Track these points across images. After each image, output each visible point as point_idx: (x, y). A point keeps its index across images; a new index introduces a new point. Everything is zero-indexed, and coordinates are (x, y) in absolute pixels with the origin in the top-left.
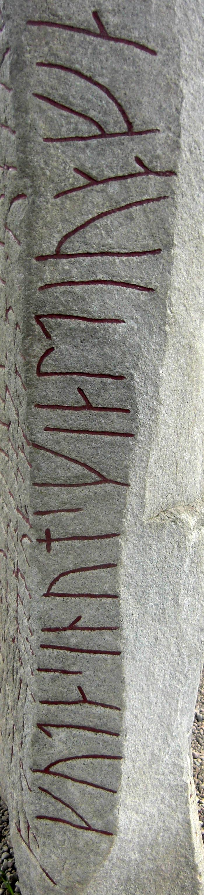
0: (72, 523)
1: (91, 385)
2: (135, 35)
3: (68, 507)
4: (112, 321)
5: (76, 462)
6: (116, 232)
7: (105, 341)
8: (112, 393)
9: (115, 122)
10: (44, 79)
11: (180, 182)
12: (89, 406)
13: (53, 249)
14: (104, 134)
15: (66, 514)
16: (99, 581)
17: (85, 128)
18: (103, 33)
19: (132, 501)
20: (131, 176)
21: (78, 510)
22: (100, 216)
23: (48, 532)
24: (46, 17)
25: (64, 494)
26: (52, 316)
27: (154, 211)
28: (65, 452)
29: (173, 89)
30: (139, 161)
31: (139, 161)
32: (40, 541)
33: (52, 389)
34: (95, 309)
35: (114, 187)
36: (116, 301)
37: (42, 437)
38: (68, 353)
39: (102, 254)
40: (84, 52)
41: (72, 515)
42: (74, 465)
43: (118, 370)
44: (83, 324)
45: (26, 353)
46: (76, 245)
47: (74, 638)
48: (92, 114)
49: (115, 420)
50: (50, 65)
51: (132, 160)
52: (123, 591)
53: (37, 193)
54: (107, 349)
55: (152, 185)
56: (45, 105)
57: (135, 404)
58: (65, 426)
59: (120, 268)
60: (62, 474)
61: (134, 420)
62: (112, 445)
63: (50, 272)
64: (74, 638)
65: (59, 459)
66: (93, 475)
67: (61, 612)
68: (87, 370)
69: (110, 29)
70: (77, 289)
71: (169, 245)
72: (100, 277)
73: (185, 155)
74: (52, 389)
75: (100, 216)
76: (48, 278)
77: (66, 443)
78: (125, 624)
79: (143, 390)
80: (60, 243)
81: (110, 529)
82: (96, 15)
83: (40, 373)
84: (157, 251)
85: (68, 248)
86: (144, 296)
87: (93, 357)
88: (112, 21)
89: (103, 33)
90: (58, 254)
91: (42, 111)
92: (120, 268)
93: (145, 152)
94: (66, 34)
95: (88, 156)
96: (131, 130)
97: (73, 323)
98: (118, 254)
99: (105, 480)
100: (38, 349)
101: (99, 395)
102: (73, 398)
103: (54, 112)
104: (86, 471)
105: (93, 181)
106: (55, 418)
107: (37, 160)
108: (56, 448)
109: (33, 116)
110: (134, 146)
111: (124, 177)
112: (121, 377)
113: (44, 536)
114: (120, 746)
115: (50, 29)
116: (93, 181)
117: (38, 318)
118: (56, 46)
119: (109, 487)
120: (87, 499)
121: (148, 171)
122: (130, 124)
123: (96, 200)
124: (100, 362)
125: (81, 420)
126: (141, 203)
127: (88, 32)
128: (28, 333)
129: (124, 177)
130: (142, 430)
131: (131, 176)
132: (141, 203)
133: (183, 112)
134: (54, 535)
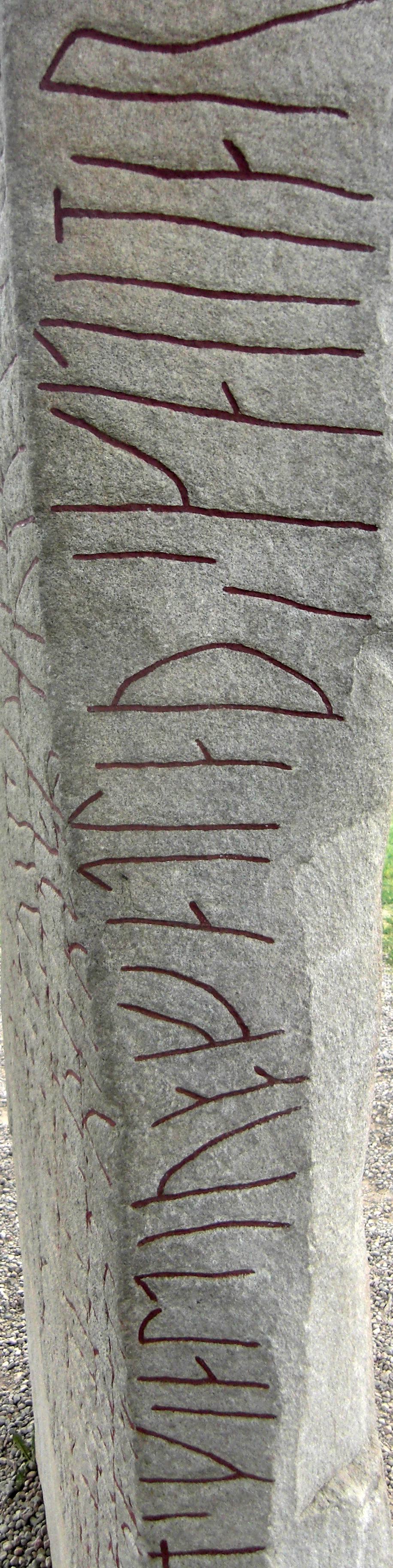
0: (197, 1533)
1: (213, 1355)
2: (245, 925)
3: (191, 1510)
4: (236, 1273)
5: (198, 1450)
6: (235, 1160)
7: (229, 1301)
8: (242, 1365)
10: (132, 986)
11: (315, 1084)
12: (212, 1379)
13: (154, 1191)
14: (212, 1044)
15: (188, 1520)
17: (188, 1039)
18: (205, 924)
20: (250, 1090)
21: (203, 1515)
22: (213, 1143)
23: (164, 1544)
24: (130, 913)
25: (185, 1495)
26: (157, 1275)
27: (284, 1128)
28: (183, 1439)
29: (298, 979)
30: (260, 1071)
31: (260, 1071)
32: (153, 1555)
33: (159, 1358)
34: (214, 1263)
35: (229, 1106)
36: (241, 1245)
37: (149, 1419)
38: (179, 1314)
39: (219, 1189)
40: (181, 950)
41: (197, 1522)
42: (195, 1455)
43: (249, 1337)
44: (199, 1282)
45: (124, 1317)
46: (183, 1182)
48: (196, 1020)
49: (250, 1400)
50: (138, 968)
51: (251, 1072)
53: (129, 1124)
54: (232, 1311)
55: (279, 1097)
56: (134, 1016)
57: (275, 1378)
58: (180, 1405)
59: (243, 1203)
60: (180, 1469)
61: (274, 1397)
62: (246, 1430)
63: (151, 1223)
65: (174, 1448)
66: (223, 1468)
68: (207, 1335)
69: (213, 919)
70: (189, 1239)
71: (307, 1165)
72: (218, 1219)
73: (320, 1050)
74: (159, 1358)
75: (213, 1143)
76: (149, 1229)
77: (183, 1427)
79: (284, 1357)
80: (163, 1182)
81: (250, 1542)
82: (194, 906)
83: (142, 1340)
84: (293, 1175)
85: (174, 1187)
86: (277, 1235)
87: (214, 1320)
88: (214, 911)
89: (205, 924)
90: (162, 1196)
91: (131, 1025)
92: (243, 1203)
93: (268, 1060)
94: (157, 930)
95: (194, 1073)
96: (247, 1036)
97: (185, 1282)
98: (241, 1187)
99: (239, 1474)
100: (140, 1312)
101: (225, 1367)
103: (147, 1024)
104: (213, 1464)
105: (202, 1100)
106: (166, 1394)
107: (128, 1085)
108: (171, 1434)
109: (120, 1032)
110: (251, 1055)
111: (242, 1092)
112: (254, 1344)
113: (158, 1549)
115: (136, 927)
116: (202, 1100)
117: (138, 1280)
118: (145, 946)
119: (247, 1484)
120: (216, 1502)
121: (272, 1081)
122: (245, 1029)
123: (207, 1123)
124: (224, 1326)
125: (202, 1396)
126: (266, 1119)
127: (186, 925)
128: (126, 1293)
129: (242, 1092)
130: (286, 1407)
131: (250, 1090)
132: (266, 1119)
133: (314, 1004)
134: (172, 1548)
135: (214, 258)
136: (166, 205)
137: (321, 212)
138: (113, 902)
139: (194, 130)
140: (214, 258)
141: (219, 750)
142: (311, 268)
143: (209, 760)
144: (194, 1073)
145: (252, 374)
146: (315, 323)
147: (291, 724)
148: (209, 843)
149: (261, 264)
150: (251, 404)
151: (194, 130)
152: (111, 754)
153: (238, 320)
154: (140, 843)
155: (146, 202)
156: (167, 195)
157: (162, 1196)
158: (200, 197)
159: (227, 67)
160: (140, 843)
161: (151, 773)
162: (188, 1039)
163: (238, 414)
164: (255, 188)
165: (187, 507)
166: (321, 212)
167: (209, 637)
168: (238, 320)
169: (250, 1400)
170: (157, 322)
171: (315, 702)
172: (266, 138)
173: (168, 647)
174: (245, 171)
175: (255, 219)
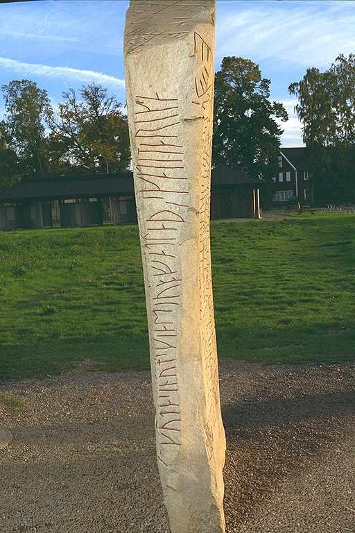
0: (164, 358)
1: (167, 326)
16: (172, 372)
17: (162, 273)
40: (159, 258)
46: (161, 295)
47: (166, 387)
59: (171, 300)
64: (166, 387)
67: (164, 380)
90: (157, 298)
92: (171, 300)
95: (162, 278)
102: (163, 329)
106: (160, 333)
123: (164, 287)
125: (166, 333)
135: (159, 156)
138: (150, 251)
139: (156, 140)
140: (159, 156)
142: (172, 157)
144: (162, 278)
151: (156, 140)
154: (155, 241)
157: (157, 298)
158: (158, 148)
159: (161, 132)
160: (155, 241)
162: (162, 273)
163: (166, 177)
168: (163, 164)
172: (166, 141)
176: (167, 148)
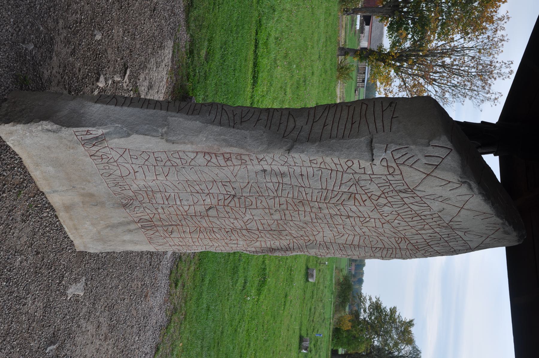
6: (225, 117)
9: (243, 120)
17: (243, 115)
19: (173, 114)
35: (232, 118)
36: (213, 116)
46: (223, 111)
52: (155, 111)
55: (232, 124)
59: (218, 117)
71: (221, 126)
78: (148, 110)
84: (220, 124)
85: (223, 111)
89: (258, 120)
90: (223, 109)
92: (218, 117)
96: (241, 122)
103: (247, 111)
114: (119, 106)
123: (231, 116)
136: (349, 118)
137: (347, 133)
141: (281, 125)
142: (341, 132)
143: (280, 124)
145: (329, 127)
146: (334, 133)
147: (283, 132)
148: (269, 122)
149: (342, 127)
150: (325, 127)
152: (283, 113)
153: (336, 125)
155: (350, 114)
156: (350, 116)
158: (350, 120)
161: (280, 117)
163: (324, 126)
164: (350, 125)
165: (313, 122)
166: (347, 133)
167: (297, 124)
168: (336, 125)
169: (190, 112)
170: (336, 116)
171: (285, 135)
172: (356, 125)
173: (296, 119)
174: (352, 124)
175: (347, 125)
176: (349, 126)
